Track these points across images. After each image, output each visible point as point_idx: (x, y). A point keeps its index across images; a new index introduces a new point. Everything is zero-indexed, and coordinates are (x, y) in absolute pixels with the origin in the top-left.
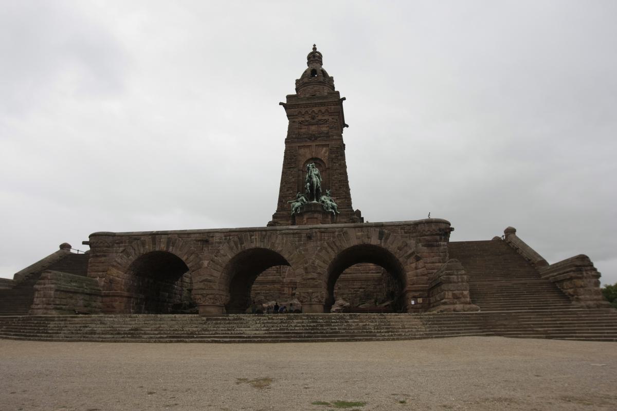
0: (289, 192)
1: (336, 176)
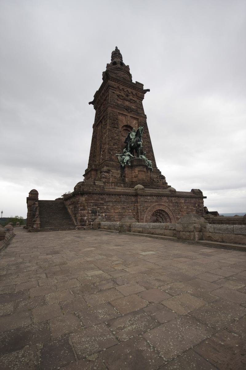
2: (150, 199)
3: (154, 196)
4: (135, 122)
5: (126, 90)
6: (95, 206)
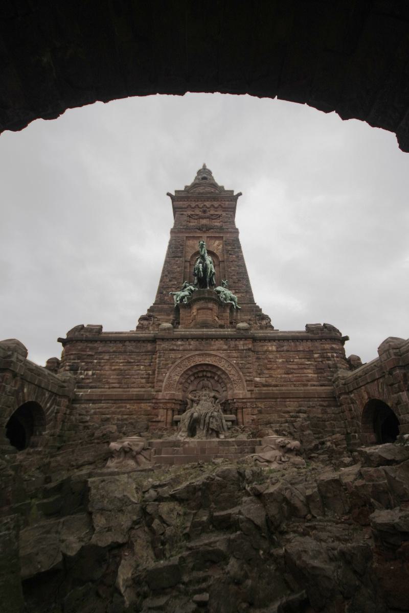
0: (172, 283)
1: (233, 268)
2: (182, 345)
3: (192, 339)
4: (217, 242)
5: (202, 205)
6: (78, 359)
